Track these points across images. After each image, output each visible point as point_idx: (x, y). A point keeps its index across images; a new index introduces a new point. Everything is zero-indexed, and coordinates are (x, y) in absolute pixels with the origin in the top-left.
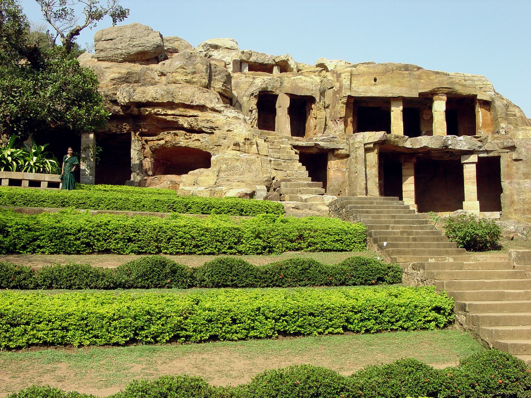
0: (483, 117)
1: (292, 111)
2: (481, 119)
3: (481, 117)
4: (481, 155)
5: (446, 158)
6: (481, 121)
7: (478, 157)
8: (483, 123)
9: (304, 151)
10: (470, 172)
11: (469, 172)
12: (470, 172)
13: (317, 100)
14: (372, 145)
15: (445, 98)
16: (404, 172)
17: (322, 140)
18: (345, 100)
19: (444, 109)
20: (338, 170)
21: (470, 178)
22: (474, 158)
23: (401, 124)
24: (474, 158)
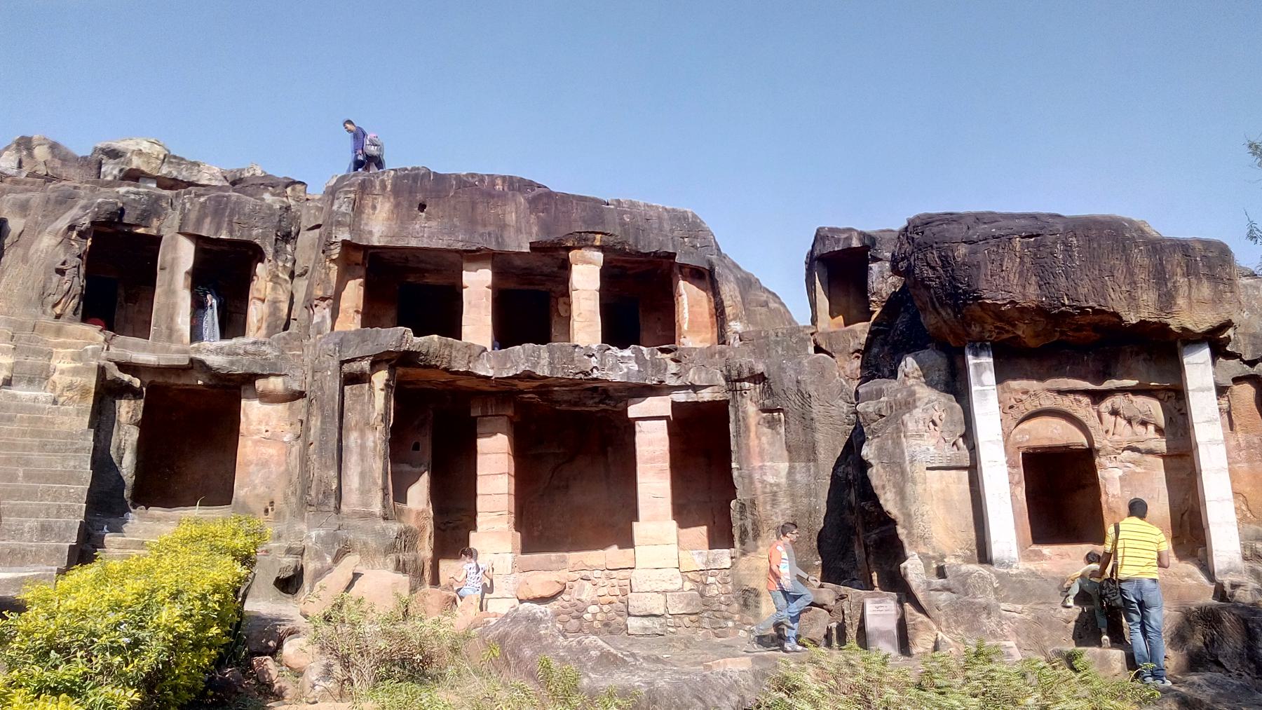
0: (691, 306)
1: (201, 279)
2: (686, 311)
3: (686, 306)
4: (681, 397)
5: (591, 406)
6: (686, 315)
7: (675, 405)
8: (691, 321)
9: (160, 380)
10: (652, 443)
11: (650, 443)
12: (652, 443)
13: (269, 251)
14: (366, 365)
15: (599, 257)
16: (483, 444)
17: (219, 351)
18: (336, 252)
19: (598, 285)
20: (272, 439)
21: (652, 459)
22: (660, 405)
23: (488, 320)
24: (660, 405)
